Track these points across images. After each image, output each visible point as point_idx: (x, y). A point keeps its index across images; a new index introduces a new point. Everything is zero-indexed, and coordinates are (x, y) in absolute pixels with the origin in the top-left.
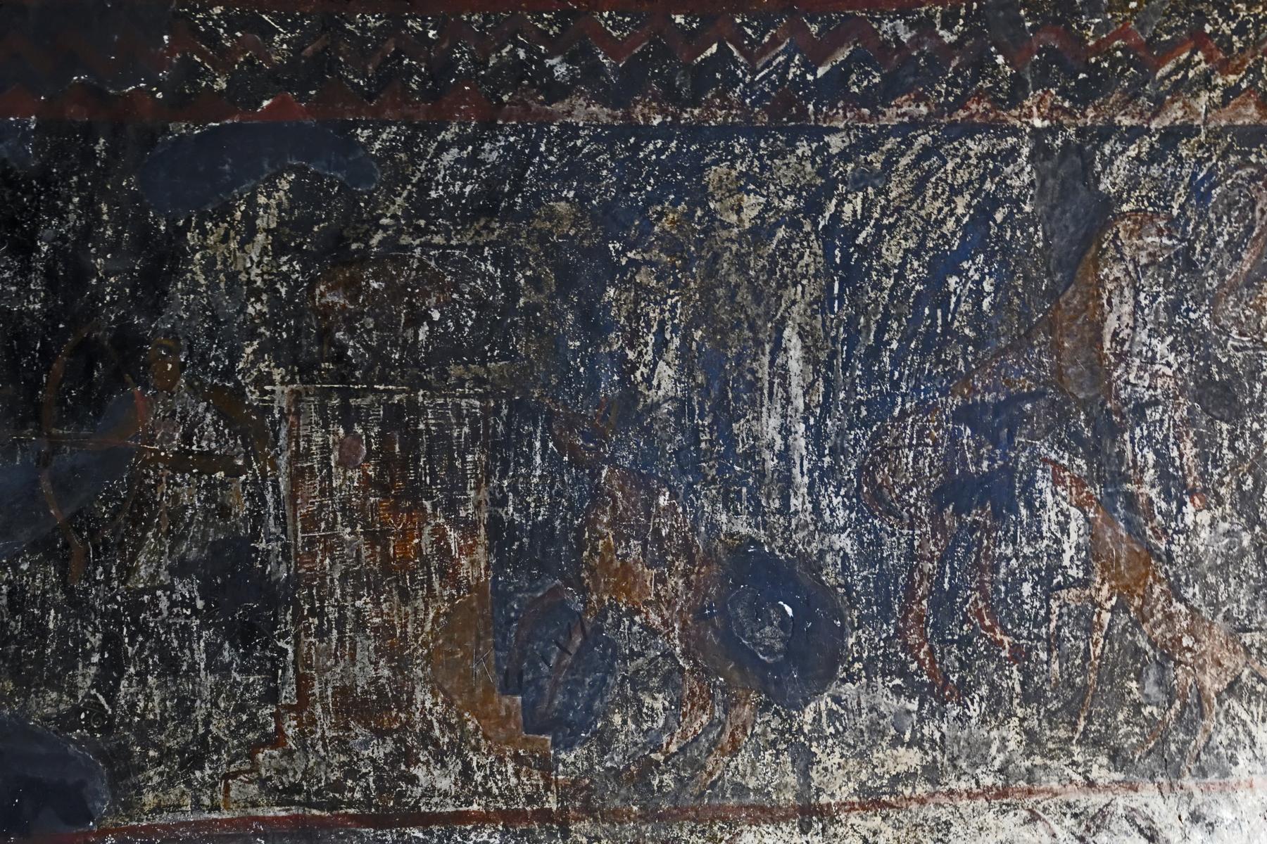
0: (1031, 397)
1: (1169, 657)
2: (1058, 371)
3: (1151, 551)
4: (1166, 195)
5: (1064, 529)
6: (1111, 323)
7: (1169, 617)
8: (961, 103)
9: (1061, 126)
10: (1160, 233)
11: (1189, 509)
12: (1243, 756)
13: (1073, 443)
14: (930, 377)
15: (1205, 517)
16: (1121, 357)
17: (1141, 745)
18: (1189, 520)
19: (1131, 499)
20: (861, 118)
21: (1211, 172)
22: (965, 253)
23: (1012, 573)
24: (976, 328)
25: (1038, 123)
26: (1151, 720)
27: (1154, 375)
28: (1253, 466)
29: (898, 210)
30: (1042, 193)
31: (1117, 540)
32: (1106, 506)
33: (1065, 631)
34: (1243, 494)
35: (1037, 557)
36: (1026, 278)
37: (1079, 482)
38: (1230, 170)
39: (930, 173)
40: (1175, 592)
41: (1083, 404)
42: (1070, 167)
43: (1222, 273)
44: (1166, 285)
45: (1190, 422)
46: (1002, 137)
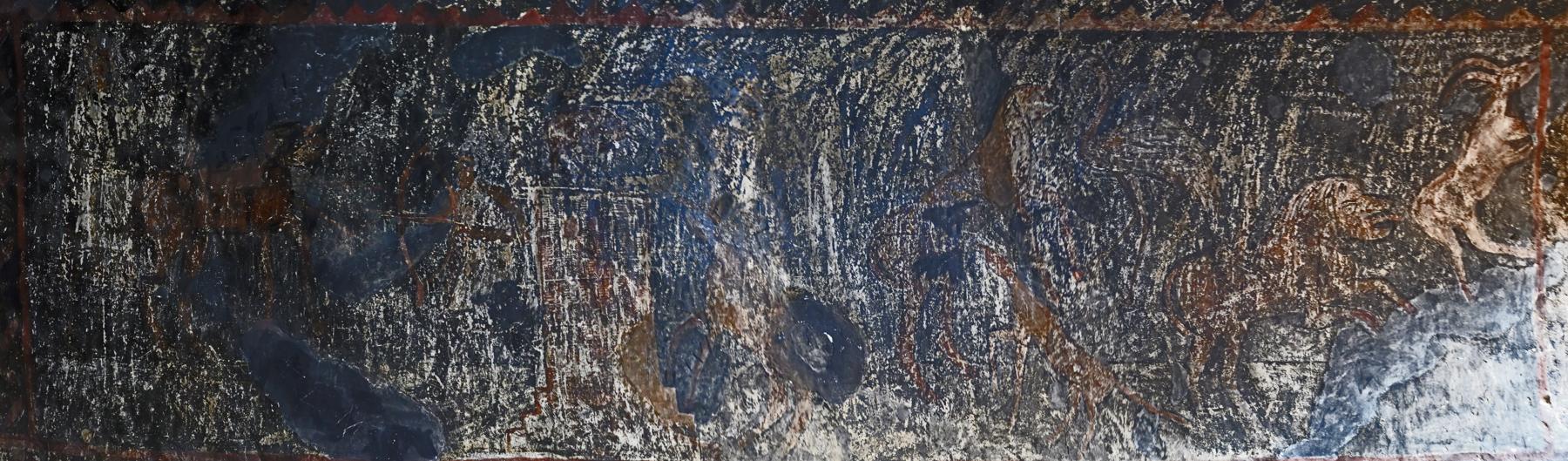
0: (970, 204)
1: (1066, 378)
2: (986, 188)
3: (1050, 307)
4: (1043, 75)
5: (995, 292)
6: (1016, 158)
7: (1064, 352)
8: (917, 15)
9: (978, 31)
10: (1042, 99)
11: (1073, 280)
12: (1115, 447)
13: (997, 235)
14: (907, 190)
15: (1083, 286)
16: (1024, 179)
17: (1051, 437)
18: (1073, 287)
19: (1036, 272)
20: (858, 24)
21: (1069, 60)
22: (924, 110)
23: (964, 318)
24: (933, 159)
25: (964, 28)
26: (1057, 420)
27: (1045, 192)
28: (1112, 253)
29: (883, 82)
30: (969, 73)
31: (1028, 299)
32: (1020, 276)
33: (1000, 358)
34: (1107, 272)
35: (979, 309)
36: (962, 127)
37: (1002, 260)
38: (1080, 59)
39: (900, 60)
40: (1066, 335)
41: (1002, 210)
42: (986, 59)
43: (1083, 126)
44: (1049, 133)
45: (1070, 222)
46: (942, 37)
